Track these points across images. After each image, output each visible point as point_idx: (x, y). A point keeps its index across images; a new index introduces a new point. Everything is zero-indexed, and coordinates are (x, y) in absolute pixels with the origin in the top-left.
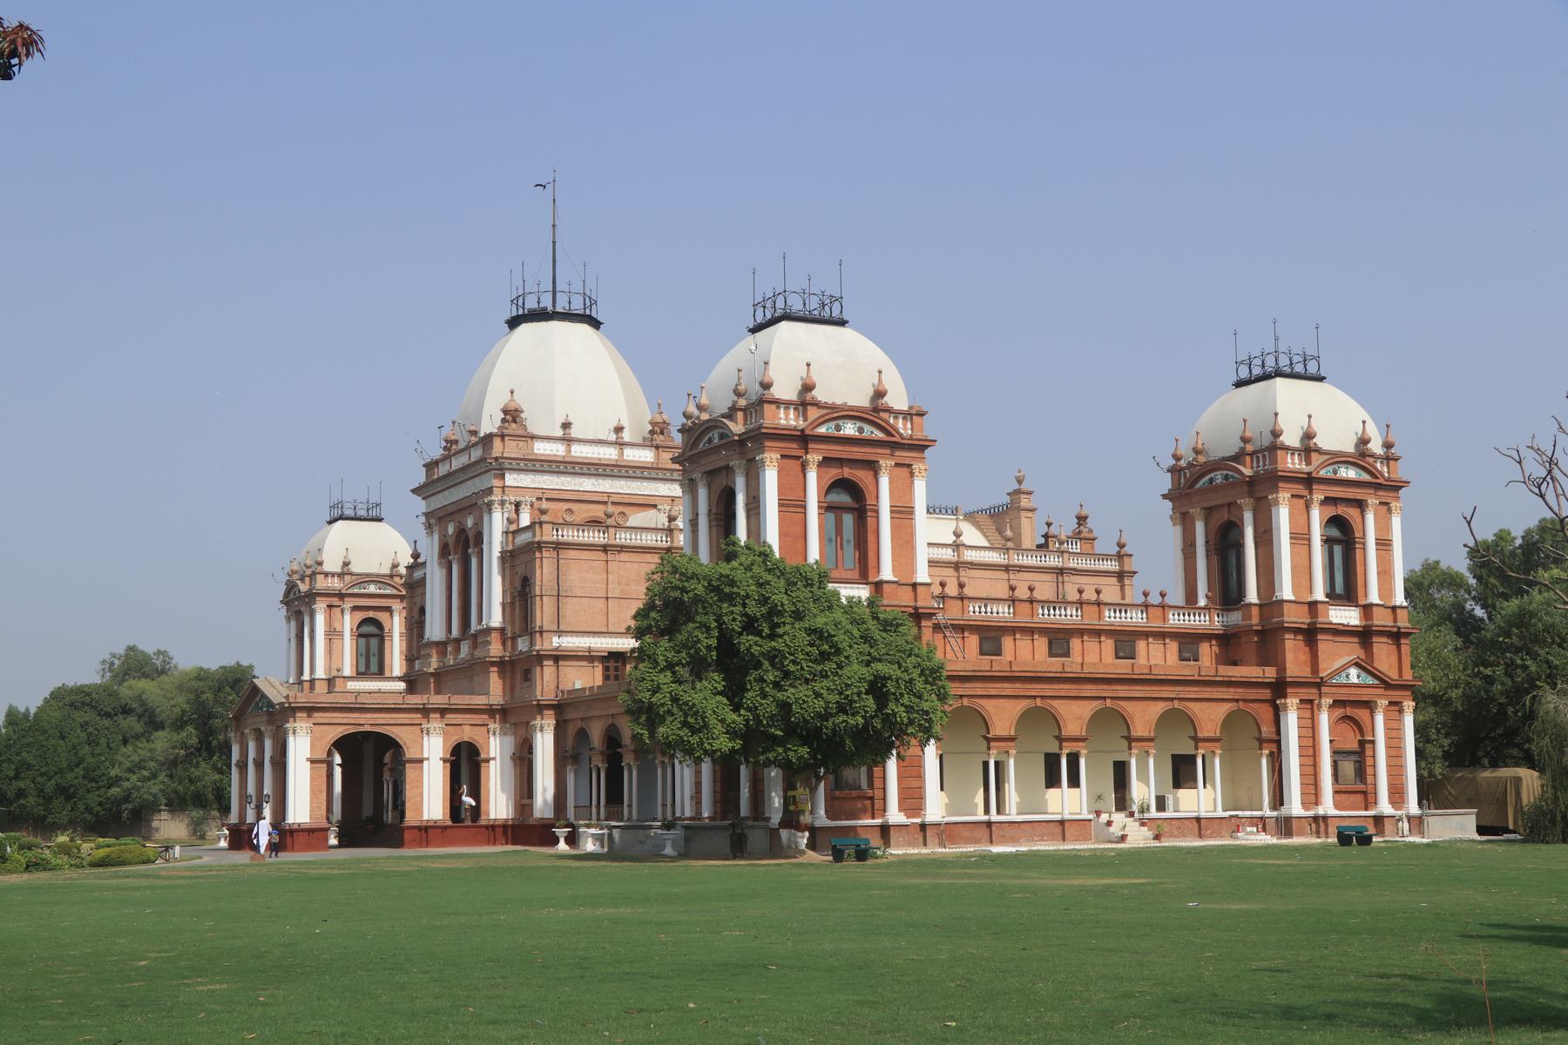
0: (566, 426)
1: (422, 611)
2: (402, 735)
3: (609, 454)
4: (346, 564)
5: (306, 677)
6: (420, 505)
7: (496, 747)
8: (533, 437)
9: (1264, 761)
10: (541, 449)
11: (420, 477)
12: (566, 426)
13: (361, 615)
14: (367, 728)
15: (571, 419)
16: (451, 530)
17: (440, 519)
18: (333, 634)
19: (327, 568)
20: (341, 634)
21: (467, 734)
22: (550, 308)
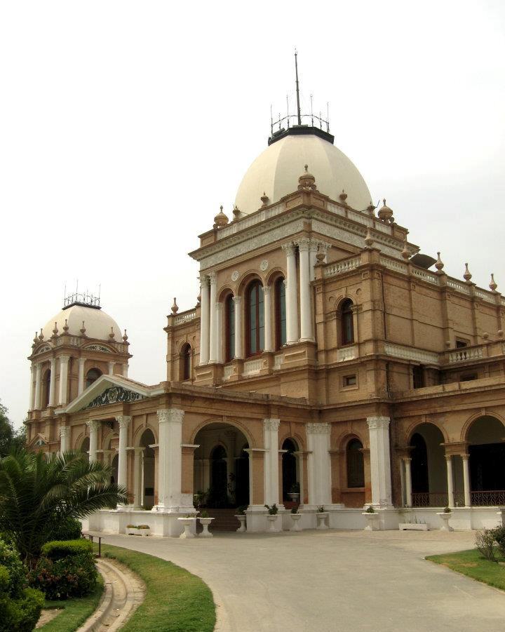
0: (343, 197)
1: (187, 347)
3: (368, 224)
4: (83, 331)
5: (50, 404)
6: (196, 266)
7: (319, 444)
8: (326, 199)
10: (331, 208)
11: (197, 245)
12: (343, 197)
13: (91, 366)
14: (225, 421)
16: (235, 277)
17: (219, 272)
18: (72, 378)
19: (71, 332)
20: (77, 377)
21: (293, 431)
22: (310, 125)
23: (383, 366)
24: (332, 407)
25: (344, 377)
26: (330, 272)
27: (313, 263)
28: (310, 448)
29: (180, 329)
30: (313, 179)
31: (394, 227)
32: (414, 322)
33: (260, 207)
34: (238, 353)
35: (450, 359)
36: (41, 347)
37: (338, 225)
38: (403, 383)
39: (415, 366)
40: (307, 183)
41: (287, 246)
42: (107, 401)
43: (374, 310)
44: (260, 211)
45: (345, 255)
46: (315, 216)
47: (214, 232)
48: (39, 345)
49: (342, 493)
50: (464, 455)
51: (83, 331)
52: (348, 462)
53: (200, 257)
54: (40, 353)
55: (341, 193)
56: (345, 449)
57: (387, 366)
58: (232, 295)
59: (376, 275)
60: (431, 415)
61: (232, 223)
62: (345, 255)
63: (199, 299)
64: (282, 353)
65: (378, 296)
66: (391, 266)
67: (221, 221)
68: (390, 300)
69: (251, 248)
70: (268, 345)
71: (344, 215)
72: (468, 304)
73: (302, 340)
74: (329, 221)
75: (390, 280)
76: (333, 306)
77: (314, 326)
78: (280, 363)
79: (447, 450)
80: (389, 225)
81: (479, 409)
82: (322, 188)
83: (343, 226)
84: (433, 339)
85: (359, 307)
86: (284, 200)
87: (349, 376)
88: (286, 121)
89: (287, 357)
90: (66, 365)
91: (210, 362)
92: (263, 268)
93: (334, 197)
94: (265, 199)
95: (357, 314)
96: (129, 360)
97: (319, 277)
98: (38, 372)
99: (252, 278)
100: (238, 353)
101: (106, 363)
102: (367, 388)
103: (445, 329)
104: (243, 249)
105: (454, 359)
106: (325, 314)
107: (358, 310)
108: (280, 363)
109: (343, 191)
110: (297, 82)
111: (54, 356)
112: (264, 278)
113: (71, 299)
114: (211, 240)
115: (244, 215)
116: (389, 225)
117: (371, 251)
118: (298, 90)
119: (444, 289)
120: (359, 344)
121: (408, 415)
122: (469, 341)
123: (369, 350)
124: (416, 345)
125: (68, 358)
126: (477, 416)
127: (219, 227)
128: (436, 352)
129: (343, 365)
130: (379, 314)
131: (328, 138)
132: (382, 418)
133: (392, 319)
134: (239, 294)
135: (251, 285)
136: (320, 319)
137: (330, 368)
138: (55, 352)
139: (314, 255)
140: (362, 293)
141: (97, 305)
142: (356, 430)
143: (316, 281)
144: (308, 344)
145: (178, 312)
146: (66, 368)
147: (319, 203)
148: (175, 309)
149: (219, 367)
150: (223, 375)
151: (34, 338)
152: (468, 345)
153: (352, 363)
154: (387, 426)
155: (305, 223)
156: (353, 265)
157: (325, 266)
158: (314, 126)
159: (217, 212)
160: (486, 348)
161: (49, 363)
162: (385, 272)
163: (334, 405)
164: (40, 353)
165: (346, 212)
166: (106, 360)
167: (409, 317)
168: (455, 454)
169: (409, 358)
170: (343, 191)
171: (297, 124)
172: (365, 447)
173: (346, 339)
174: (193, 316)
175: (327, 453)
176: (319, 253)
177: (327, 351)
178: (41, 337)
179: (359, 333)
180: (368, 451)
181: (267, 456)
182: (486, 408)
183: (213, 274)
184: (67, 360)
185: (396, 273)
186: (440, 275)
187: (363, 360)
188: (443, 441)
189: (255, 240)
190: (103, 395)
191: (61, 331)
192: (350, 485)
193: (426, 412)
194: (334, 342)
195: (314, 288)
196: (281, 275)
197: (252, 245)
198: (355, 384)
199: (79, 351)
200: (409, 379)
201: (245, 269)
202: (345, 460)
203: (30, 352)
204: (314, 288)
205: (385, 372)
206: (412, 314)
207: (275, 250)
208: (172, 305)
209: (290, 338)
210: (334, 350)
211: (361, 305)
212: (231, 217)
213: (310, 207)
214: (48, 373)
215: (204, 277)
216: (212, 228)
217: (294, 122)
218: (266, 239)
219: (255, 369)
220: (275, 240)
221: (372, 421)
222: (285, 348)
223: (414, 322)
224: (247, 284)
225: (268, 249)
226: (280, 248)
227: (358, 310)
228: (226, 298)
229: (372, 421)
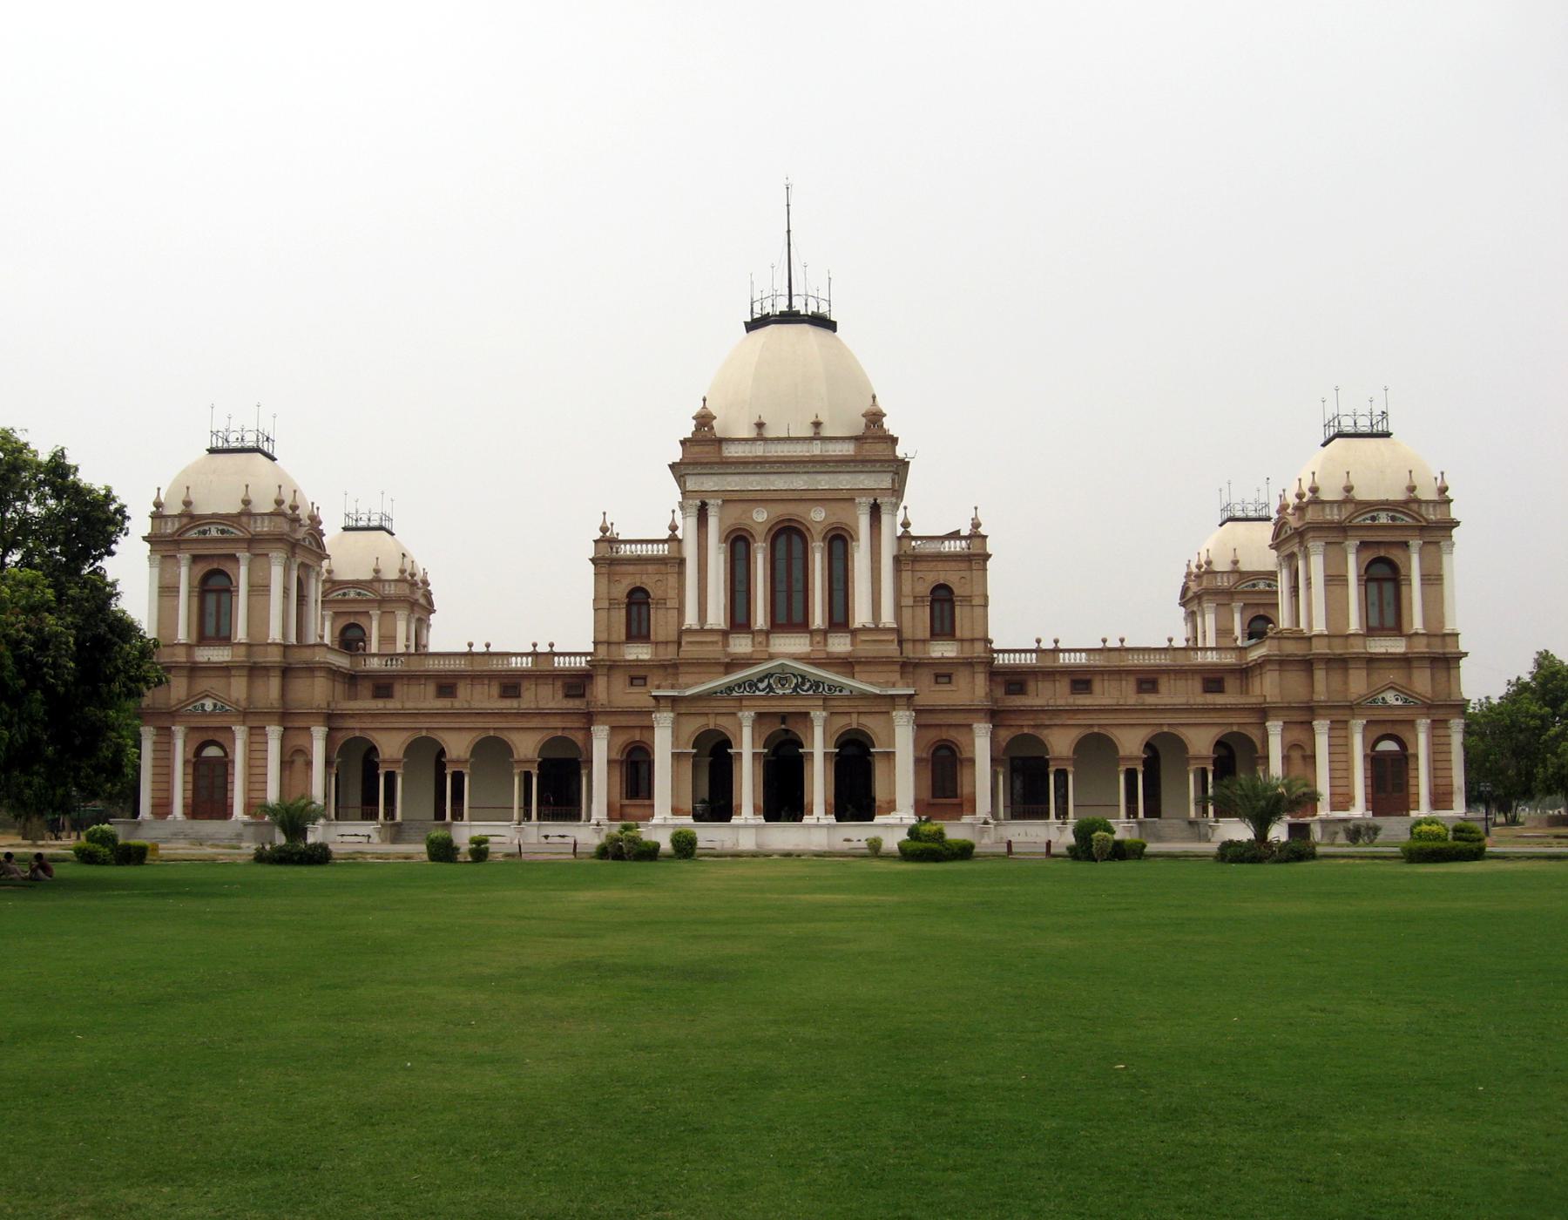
5: (241, 634)
9: (1191, 777)
16: (761, 517)
34: (760, 619)
41: (864, 503)
42: (769, 685)
49: (929, 805)
54: (193, 534)
63: (673, 528)
70: (818, 619)
76: (924, 589)
77: (898, 607)
78: (840, 645)
87: (943, 673)
92: (818, 516)
100: (760, 619)
104: (779, 483)
108: (840, 645)
135: (788, 535)
136: (908, 601)
142: (952, 735)
148: (604, 529)
150: (726, 644)
151: (154, 498)
159: (697, 408)
164: (193, 534)
177: (914, 641)
180: (972, 761)
189: (805, 477)
190: (761, 680)
194: (923, 631)
197: (799, 482)
201: (782, 511)
209: (861, 615)
218: (824, 482)
219: (790, 645)
228: (738, 542)
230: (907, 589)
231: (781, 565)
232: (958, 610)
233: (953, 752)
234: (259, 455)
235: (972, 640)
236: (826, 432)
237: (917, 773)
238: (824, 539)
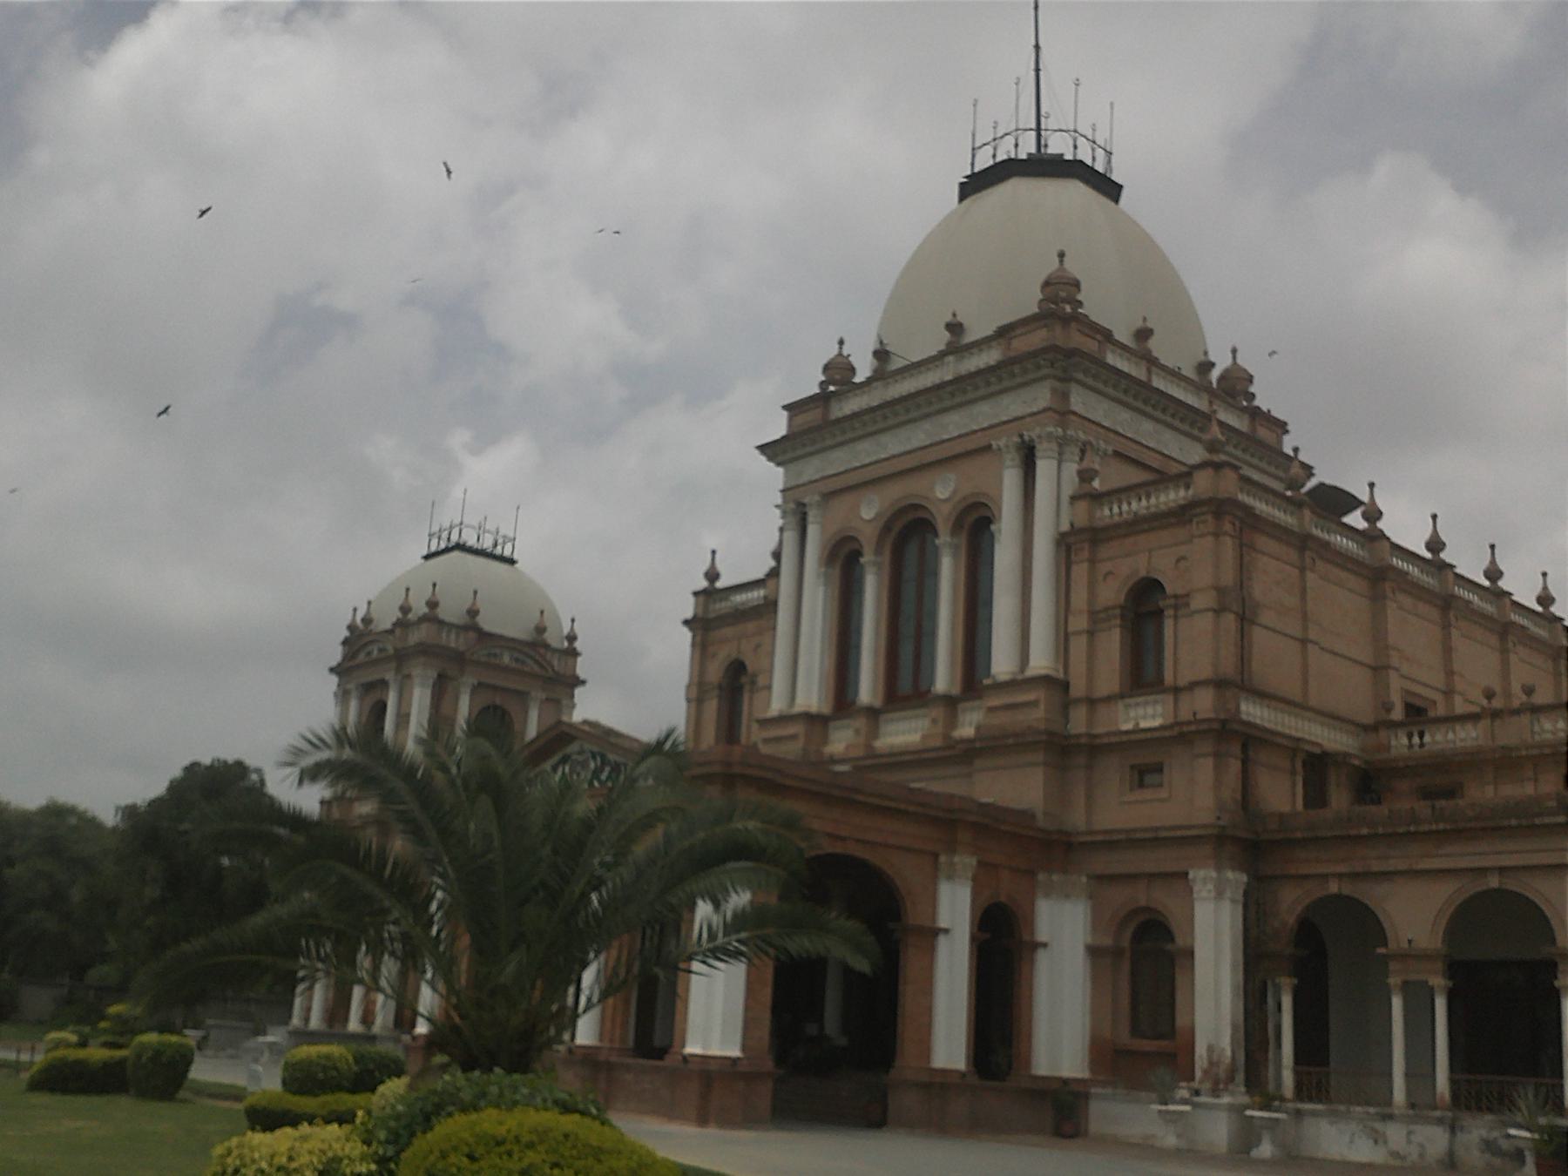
0: (1144, 334)
1: (737, 669)
2: (903, 871)
4: (473, 613)
6: (774, 476)
8: (1107, 336)
11: (778, 428)
12: (1144, 334)
15: (1149, 325)
16: (870, 510)
22: (1069, 157)
23: (1236, 749)
24: (1099, 838)
25: (1132, 767)
26: (1107, 514)
27: (1067, 491)
28: (1042, 934)
29: (726, 622)
30: (1077, 285)
31: (1256, 414)
32: (1310, 646)
33: (942, 347)
34: (867, 690)
35: (1393, 743)
36: (366, 645)
37: (1130, 400)
38: (1280, 793)
39: (1311, 755)
40: (1060, 297)
41: (1004, 441)
43: (1218, 611)
44: (942, 355)
45: (1144, 476)
46: (1080, 376)
47: (822, 399)
48: (359, 639)
50: (1438, 982)
51: (473, 613)
52: (1134, 974)
53: (780, 459)
55: (1139, 324)
56: (1126, 943)
57: (1245, 747)
58: (856, 555)
59: (1228, 527)
60: (1355, 876)
61: (869, 381)
62: (1144, 476)
63: (777, 555)
64: (980, 697)
65: (1228, 577)
66: (1261, 507)
67: (838, 370)
68: (1258, 590)
69: (915, 444)
70: (944, 678)
71: (1144, 378)
72: (1434, 614)
73: (1029, 673)
74: (1110, 391)
75: (1262, 541)
76: (1112, 593)
77: (1063, 639)
79: (1393, 966)
80: (1244, 410)
81: (1483, 871)
82: (1095, 305)
83: (1139, 404)
84: (1350, 690)
85: (1181, 601)
86: (1004, 332)
87: (1145, 761)
88: (1010, 140)
89: (991, 710)
90: (428, 692)
91: (797, 709)
92: (943, 491)
93: (1123, 335)
94: (955, 328)
95: (1176, 617)
96: (578, 691)
97: (1082, 521)
98: (353, 705)
99: (911, 516)
100: (867, 690)
101: (522, 696)
102: (1195, 793)
103: (1379, 670)
105: (1400, 743)
106: (1093, 614)
107: (1176, 608)
109: (1145, 319)
110: (1037, 47)
111: (398, 670)
112: (943, 518)
113: (445, 535)
114: (812, 417)
115: (896, 364)
116: (1244, 410)
117: (1218, 467)
118: (1037, 70)
119: (1381, 571)
120: (1176, 690)
121: (1293, 872)
122: (1435, 703)
123: (1203, 704)
124: (1313, 702)
125: (432, 674)
126: (1473, 887)
127: (832, 388)
128: (1357, 725)
129: (1133, 737)
130: (1229, 620)
131: (1110, 189)
132: (1230, 875)
133: (1258, 635)
134: (878, 551)
135: (909, 531)
136: (1079, 623)
137: (1098, 741)
138: (401, 658)
139: (1071, 468)
140: (1194, 565)
141: (507, 553)
143: (1074, 531)
144: (1046, 680)
145: (719, 584)
146: (428, 701)
147: (1090, 345)
148: (712, 575)
149: (816, 722)
150: (825, 740)
151: (348, 620)
152: (1431, 714)
153: (1157, 734)
154: (1240, 897)
155: (1054, 391)
156: (1173, 497)
157: (1097, 498)
158: (1079, 157)
160: (1488, 721)
161: (383, 684)
162: (1251, 522)
163: (1106, 832)
164: (361, 657)
165: (1149, 372)
166: (520, 687)
167: (1299, 634)
168: (1413, 977)
169: (1299, 735)
170: (1145, 319)
171: (1033, 150)
172: (1180, 941)
173: (1142, 675)
174: (756, 595)
175: (1080, 952)
176: (1085, 464)
177: (1092, 702)
178: (367, 620)
179: (1176, 662)
180: (1190, 954)
181: (942, 943)
182: (1502, 870)
183: (817, 498)
184: (431, 682)
185: (1276, 526)
186: (1374, 537)
187: (1185, 729)
188: (1386, 945)
189: (926, 425)
190: (555, 769)
191: (420, 608)
192: (1135, 1031)
193: (1342, 868)
194: (1109, 678)
195: (1068, 549)
196: (984, 512)
198: (1161, 785)
199: (460, 659)
200: (1294, 785)
201: (895, 493)
202: (1126, 966)
203: (336, 655)
204: (1068, 549)
205: (1239, 764)
206: (1305, 629)
207: (977, 450)
208: (706, 566)
209: (1002, 664)
210: (1109, 699)
211: (1187, 595)
212: (864, 368)
213: (1072, 353)
214: (381, 708)
215: (792, 505)
216: (817, 391)
217: (1028, 147)
218: (954, 424)
219: (905, 733)
220: (975, 428)
221: (1203, 879)
222: (989, 687)
223: (1310, 646)
224: (897, 528)
225: (958, 448)
226: (989, 447)
227: (1176, 608)
228: (844, 560)
229: (1203, 879)
230: (1079, 598)
231: (909, 591)
232: (1168, 625)
233: (1169, 935)
234: (456, 554)
235: (1193, 686)
236: (969, 338)
237: (1096, 978)
238: (957, 527)
